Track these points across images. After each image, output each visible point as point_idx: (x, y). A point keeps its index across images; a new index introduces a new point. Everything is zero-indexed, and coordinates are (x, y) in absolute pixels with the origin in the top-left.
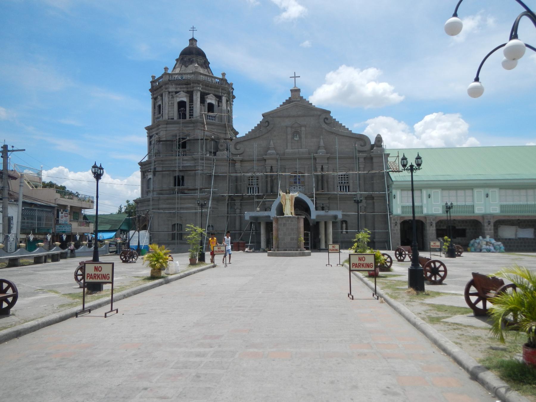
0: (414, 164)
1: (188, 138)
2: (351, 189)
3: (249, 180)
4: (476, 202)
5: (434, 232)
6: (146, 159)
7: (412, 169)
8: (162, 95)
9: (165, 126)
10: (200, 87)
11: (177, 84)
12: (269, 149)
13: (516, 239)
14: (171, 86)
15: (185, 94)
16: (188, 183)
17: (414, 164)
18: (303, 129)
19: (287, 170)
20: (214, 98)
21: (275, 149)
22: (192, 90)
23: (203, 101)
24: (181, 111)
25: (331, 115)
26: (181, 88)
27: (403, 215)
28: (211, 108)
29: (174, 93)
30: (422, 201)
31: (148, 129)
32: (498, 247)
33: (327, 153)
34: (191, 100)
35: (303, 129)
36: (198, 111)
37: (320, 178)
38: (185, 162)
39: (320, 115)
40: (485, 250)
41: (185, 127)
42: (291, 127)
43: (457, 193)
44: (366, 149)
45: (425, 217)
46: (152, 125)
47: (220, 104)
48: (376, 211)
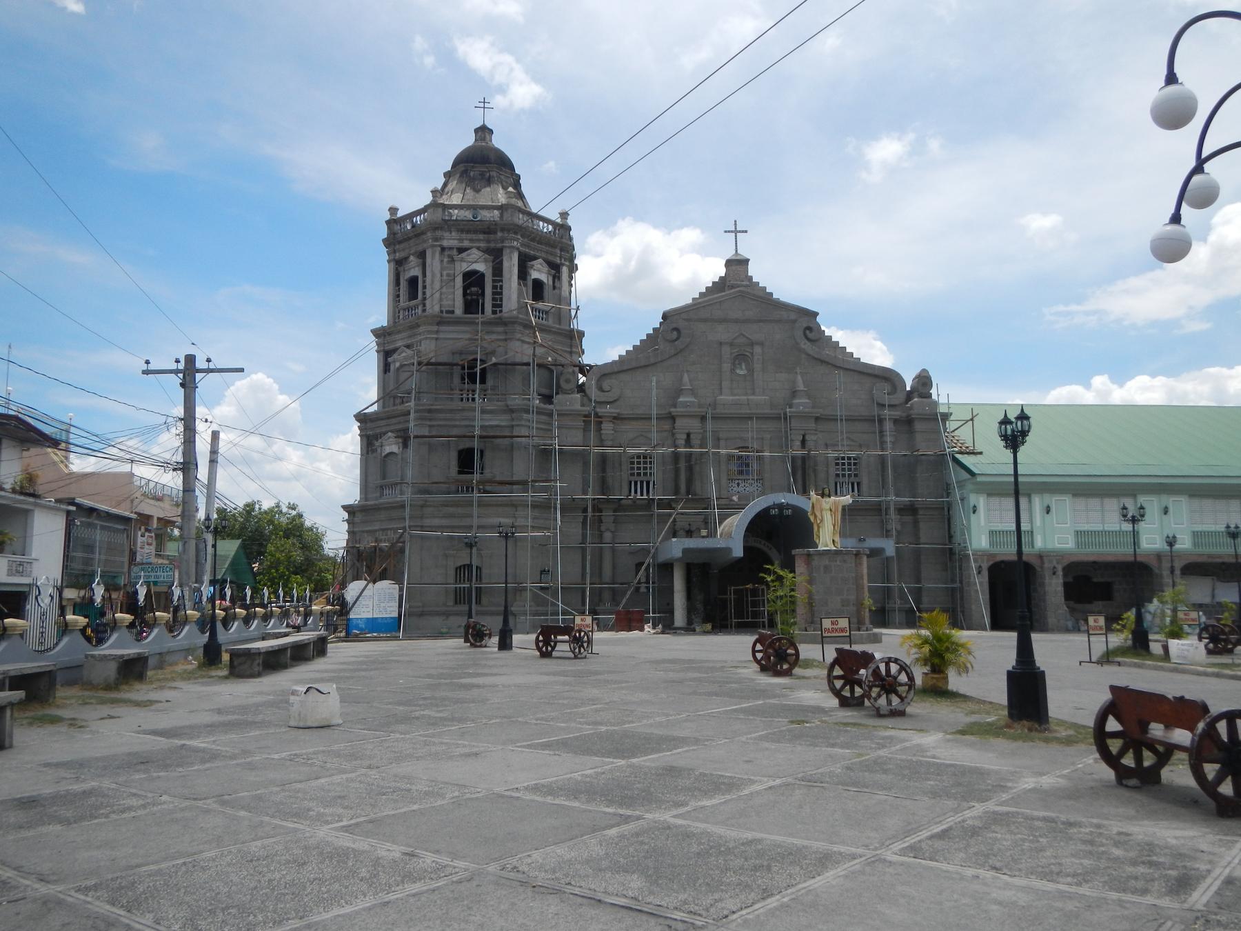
1: (494, 360)
2: (864, 487)
3: (632, 463)
5: (1060, 589)
6: (375, 408)
8: (422, 255)
9: (435, 328)
10: (517, 240)
11: (462, 231)
12: (679, 392)
13: (1213, 606)
14: (447, 234)
15: (480, 254)
16: (495, 467)
18: (758, 349)
19: (722, 443)
20: (546, 268)
21: (693, 392)
22: (499, 245)
23: (523, 274)
24: (471, 294)
25: (818, 319)
26: (471, 240)
27: (996, 550)
28: (538, 290)
29: (455, 252)
30: (1031, 522)
31: (379, 333)
33: (813, 407)
34: (498, 271)
35: (758, 349)
36: (514, 296)
37: (799, 463)
38: (486, 416)
39: (794, 321)
41: (488, 333)
42: (731, 344)
43: (1102, 506)
44: (896, 402)
45: (1040, 556)
46: (389, 327)
47: (557, 284)
48: (922, 540)
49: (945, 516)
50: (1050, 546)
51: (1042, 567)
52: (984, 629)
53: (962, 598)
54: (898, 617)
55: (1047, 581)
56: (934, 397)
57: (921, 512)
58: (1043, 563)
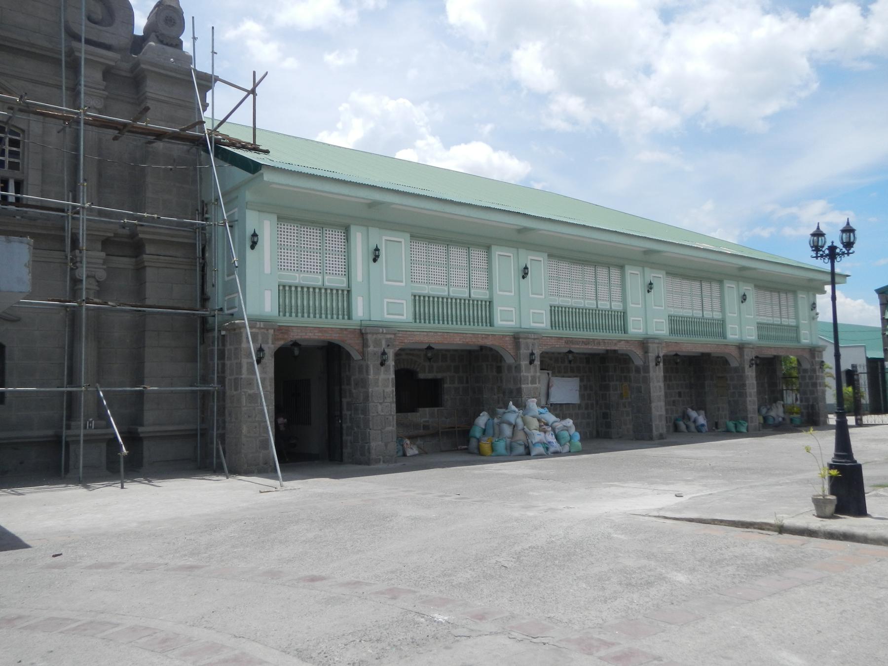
4: (498, 293)
5: (391, 389)
27: (287, 321)
30: (348, 273)
32: (566, 434)
40: (540, 449)
45: (362, 333)
49: (197, 255)
50: (376, 317)
51: (363, 354)
52: (264, 469)
53: (222, 411)
54: (81, 455)
55: (371, 376)
56: (187, 46)
57: (149, 249)
58: (365, 344)
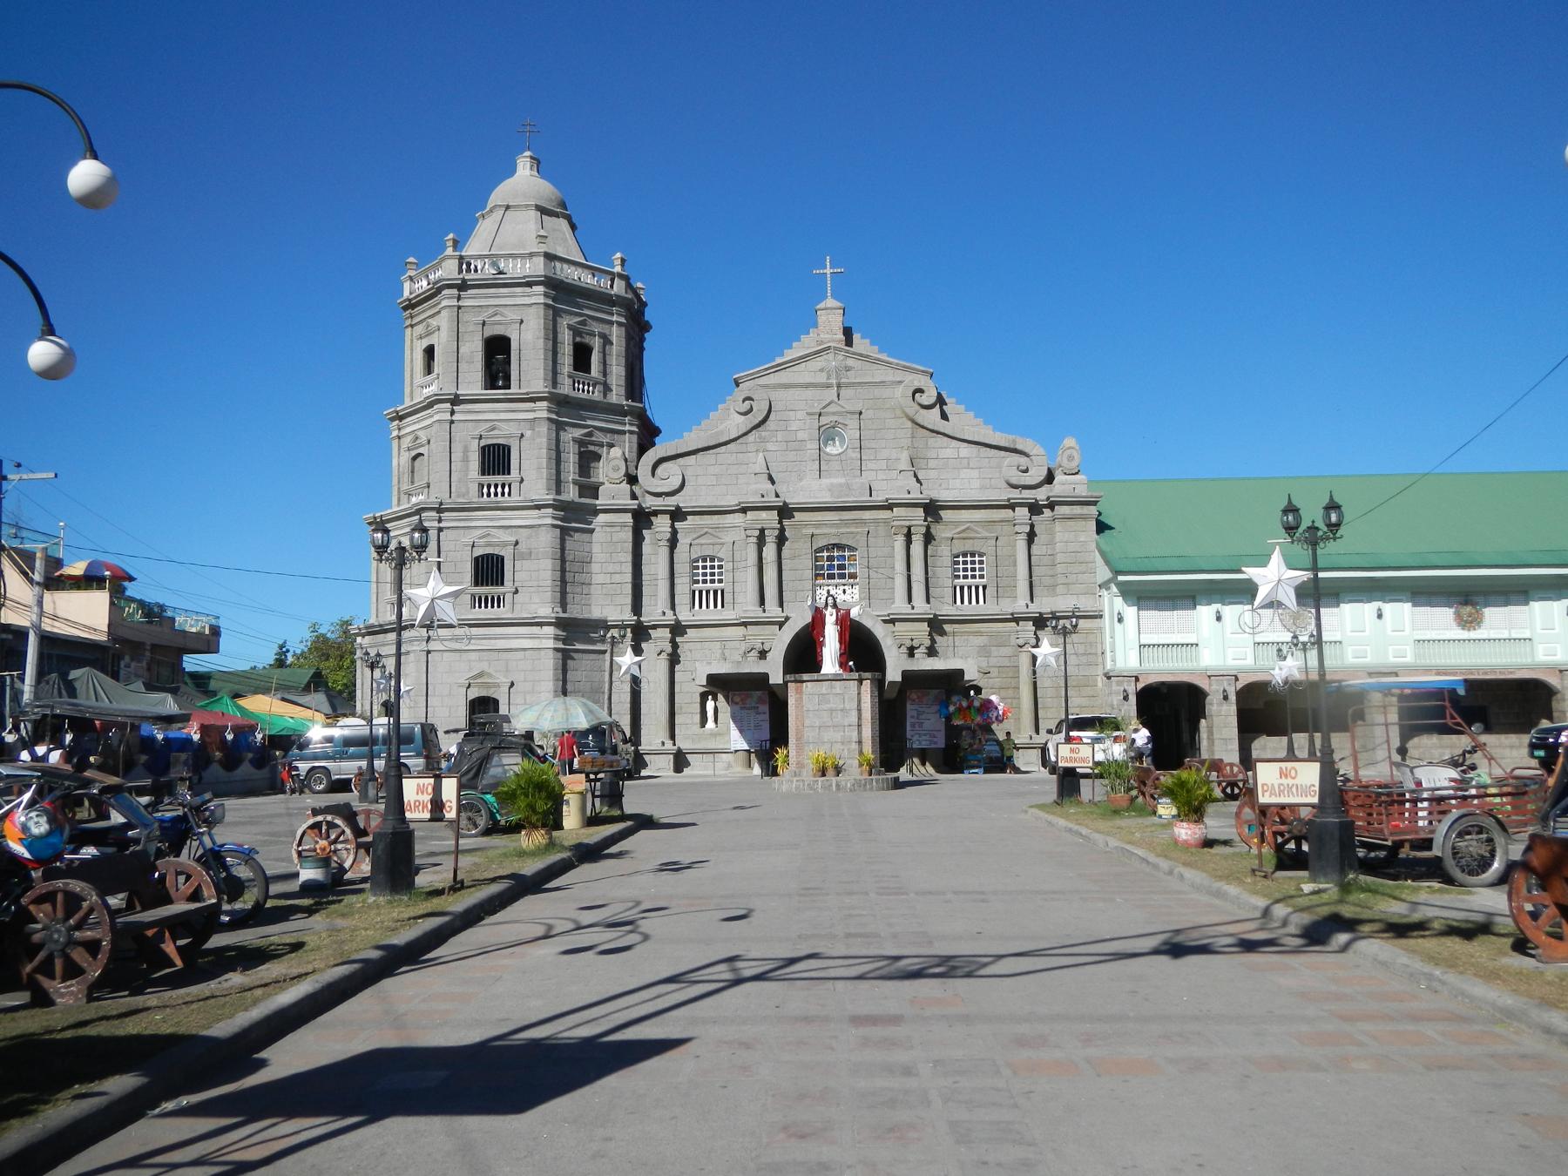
0: (1320, 524)
7: (1313, 539)
17: (1320, 524)
